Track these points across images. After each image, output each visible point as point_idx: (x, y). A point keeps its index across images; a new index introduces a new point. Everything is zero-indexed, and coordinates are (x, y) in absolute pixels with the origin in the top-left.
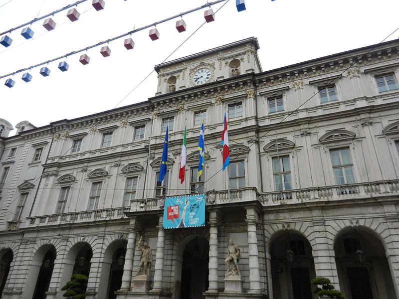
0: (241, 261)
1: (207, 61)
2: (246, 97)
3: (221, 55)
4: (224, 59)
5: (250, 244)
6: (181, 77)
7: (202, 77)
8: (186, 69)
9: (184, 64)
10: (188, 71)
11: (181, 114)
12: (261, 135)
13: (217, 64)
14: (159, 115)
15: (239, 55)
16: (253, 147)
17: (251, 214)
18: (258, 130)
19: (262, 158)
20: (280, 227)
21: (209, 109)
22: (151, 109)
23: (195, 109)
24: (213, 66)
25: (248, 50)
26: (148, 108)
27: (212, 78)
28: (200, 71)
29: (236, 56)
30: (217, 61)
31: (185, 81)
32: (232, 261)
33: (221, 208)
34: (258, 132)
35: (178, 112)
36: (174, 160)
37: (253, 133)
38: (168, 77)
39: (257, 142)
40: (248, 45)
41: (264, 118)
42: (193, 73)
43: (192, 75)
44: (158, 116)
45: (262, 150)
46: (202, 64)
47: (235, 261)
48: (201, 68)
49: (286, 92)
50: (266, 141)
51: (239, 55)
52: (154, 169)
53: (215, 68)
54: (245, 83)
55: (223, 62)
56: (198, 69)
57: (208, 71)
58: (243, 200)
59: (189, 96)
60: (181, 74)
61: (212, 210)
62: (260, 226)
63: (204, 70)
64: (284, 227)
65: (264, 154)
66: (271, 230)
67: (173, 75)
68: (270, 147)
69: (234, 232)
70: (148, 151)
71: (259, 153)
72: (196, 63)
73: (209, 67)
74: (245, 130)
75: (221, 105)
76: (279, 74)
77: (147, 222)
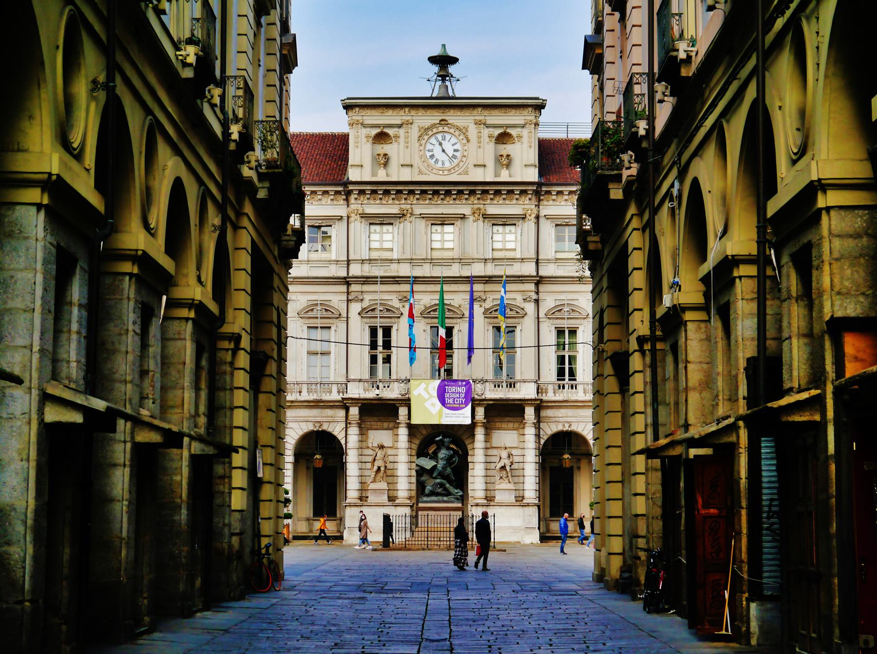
0: (515, 466)
2: (523, 218)
5: (522, 445)
6: (402, 140)
11: (407, 224)
12: (542, 288)
13: (473, 131)
14: (364, 216)
16: (530, 308)
17: (530, 412)
18: (539, 281)
19: (541, 325)
21: (458, 223)
24: (463, 131)
27: (464, 159)
28: (439, 136)
29: (508, 126)
32: (503, 468)
34: (537, 284)
37: (532, 287)
38: (375, 131)
39: (537, 301)
41: (549, 261)
42: (426, 137)
45: (542, 315)
47: (508, 468)
48: (441, 129)
50: (548, 302)
52: (365, 320)
53: (468, 141)
54: (523, 192)
55: (486, 132)
56: (435, 130)
57: (454, 140)
59: (424, 192)
60: (401, 132)
61: (479, 405)
62: (537, 426)
63: (448, 136)
66: (549, 429)
67: (386, 130)
69: (499, 429)
70: (348, 284)
74: (520, 279)
77: (379, 412)
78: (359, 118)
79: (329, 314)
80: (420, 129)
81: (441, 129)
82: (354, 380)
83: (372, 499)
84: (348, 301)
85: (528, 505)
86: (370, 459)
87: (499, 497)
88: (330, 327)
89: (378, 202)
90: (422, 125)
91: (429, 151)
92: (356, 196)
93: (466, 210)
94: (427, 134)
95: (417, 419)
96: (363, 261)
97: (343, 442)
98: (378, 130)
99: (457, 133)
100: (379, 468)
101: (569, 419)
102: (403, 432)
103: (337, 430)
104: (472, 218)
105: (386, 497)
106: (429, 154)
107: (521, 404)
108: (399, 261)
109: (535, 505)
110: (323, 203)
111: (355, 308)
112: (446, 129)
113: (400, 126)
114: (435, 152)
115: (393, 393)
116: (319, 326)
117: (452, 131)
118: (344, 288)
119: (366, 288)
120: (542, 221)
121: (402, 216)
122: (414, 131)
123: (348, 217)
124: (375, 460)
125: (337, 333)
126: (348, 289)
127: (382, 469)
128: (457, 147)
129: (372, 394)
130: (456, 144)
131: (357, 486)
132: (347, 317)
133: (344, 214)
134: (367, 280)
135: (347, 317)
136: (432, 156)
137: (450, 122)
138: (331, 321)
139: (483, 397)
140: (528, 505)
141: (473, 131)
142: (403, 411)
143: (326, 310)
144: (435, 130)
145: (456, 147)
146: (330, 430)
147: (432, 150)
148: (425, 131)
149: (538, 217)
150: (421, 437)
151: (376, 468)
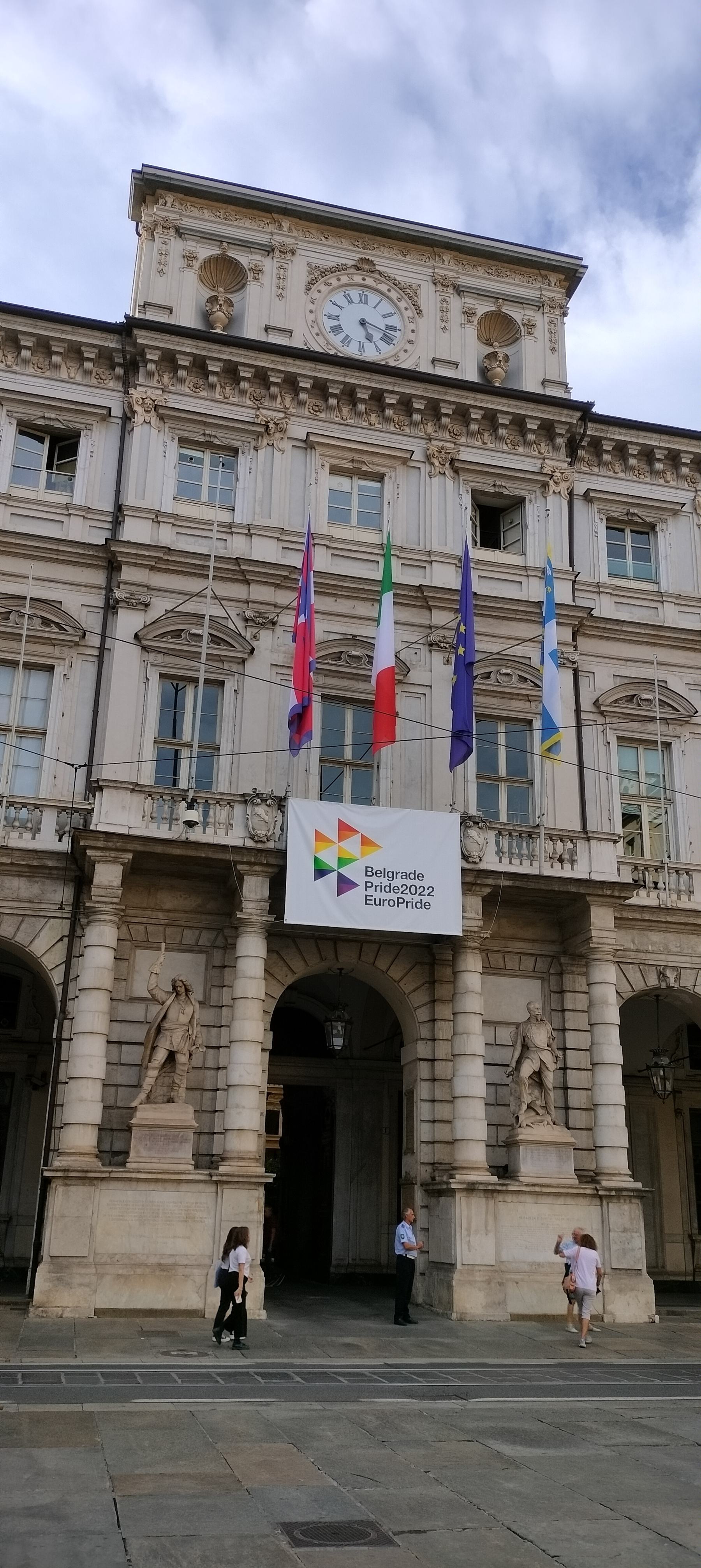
1: (389, 261)
3: (448, 267)
4: (459, 291)
7: (363, 323)
8: (293, 253)
9: (286, 224)
10: (298, 271)
12: (584, 644)
13: (428, 296)
15: (520, 302)
18: (583, 624)
20: (653, 981)
22: (119, 371)
23: (340, 453)
24: (409, 293)
25: (552, 300)
26: (105, 357)
27: (408, 347)
28: (355, 294)
30: (432, 287)
31: (279, 305)
32: (538, 1078)
33: (509, 887)
35: (260, 435)
36: (255, 644)
40: (554, 278)
43: (316, 295)
44: (162, 418)
45: (586, 704)
46: (364, 266)
48: (358, 279)
49: (670, 521)
50: (602, 679)
51: (520, 302)
52: (151, 657)
53: (419, 312)
55: (456, 304)
56: (345, 279)
58: (580, 872)
59: (321, 388)
60: (269, 265)
63: (373, 298)
64: (662, 975)
65: (592, 717)
67: (232, 253)
68: (616, 701)
70: (113, 566)
71: (578, 711)
72: (337, 252)
73: (394, 295)
75: (450, 483)
76: (659, 448)
78: (172, 216)
79: (52, 632)
80: (312, 268)
81: (358, 279)
82: (116, 785)
83: (141, 1155)
84: (110, 608)
85: (619, 1194)
86: (139, 1034)
87: (530, 1166)
88: (50, 669)
89: (204, 394)
90: (316, 262)
91: (330, 317)
92: (151, 367)
93: (417, 447)
94: (327, 284)
95: (309, 904)
96: (157, 517)
97: (57, 977)
98: (214, 251)
99: (394, 295)
100: (171, 1056)
101: (674, 960)
102: (252, 949)
103: (44, 944)
104: (425, 468)
105: (186, 1153)
106: (329, 323)
107: (583, 895)
108: (249, 532)
109: (638, 1195)
110: (64, 374)
111: (128, 622)
112: (369, 281)
113: (269, 250)
114: (342, 322)
115: (227, 831)
116: (22, 658)
117: (383, 288)
118: (98, 578)
119: (159, 580)
120: (578, 504)
121: (265, 431)
122: (298, 271)
123: (127, 418)
124: (159, 1030)
125: (74, 679)
126: (109, 580)
127: (182, 1058)
128: (394, 321)
129: (162, 832)
130: (391, 315)
131: (93, 1113)
132: (102, 649)
133: (117, 412)
134: (162, 559)
135: (102, 649)
136: (337, 329)
137: (378, 268)
138: (57, 651)
139: (483, 866)
140: (619, 1194)
141: (428, 296)
142: (254, 890)
143: (46, 622)
144: (345, 279)
145: (391, 321)
146: (21, 938)
147: (337, 318)
148: (318, 275)
149: (571, 494)
150: (290, 980)
151: (161, 1055)
